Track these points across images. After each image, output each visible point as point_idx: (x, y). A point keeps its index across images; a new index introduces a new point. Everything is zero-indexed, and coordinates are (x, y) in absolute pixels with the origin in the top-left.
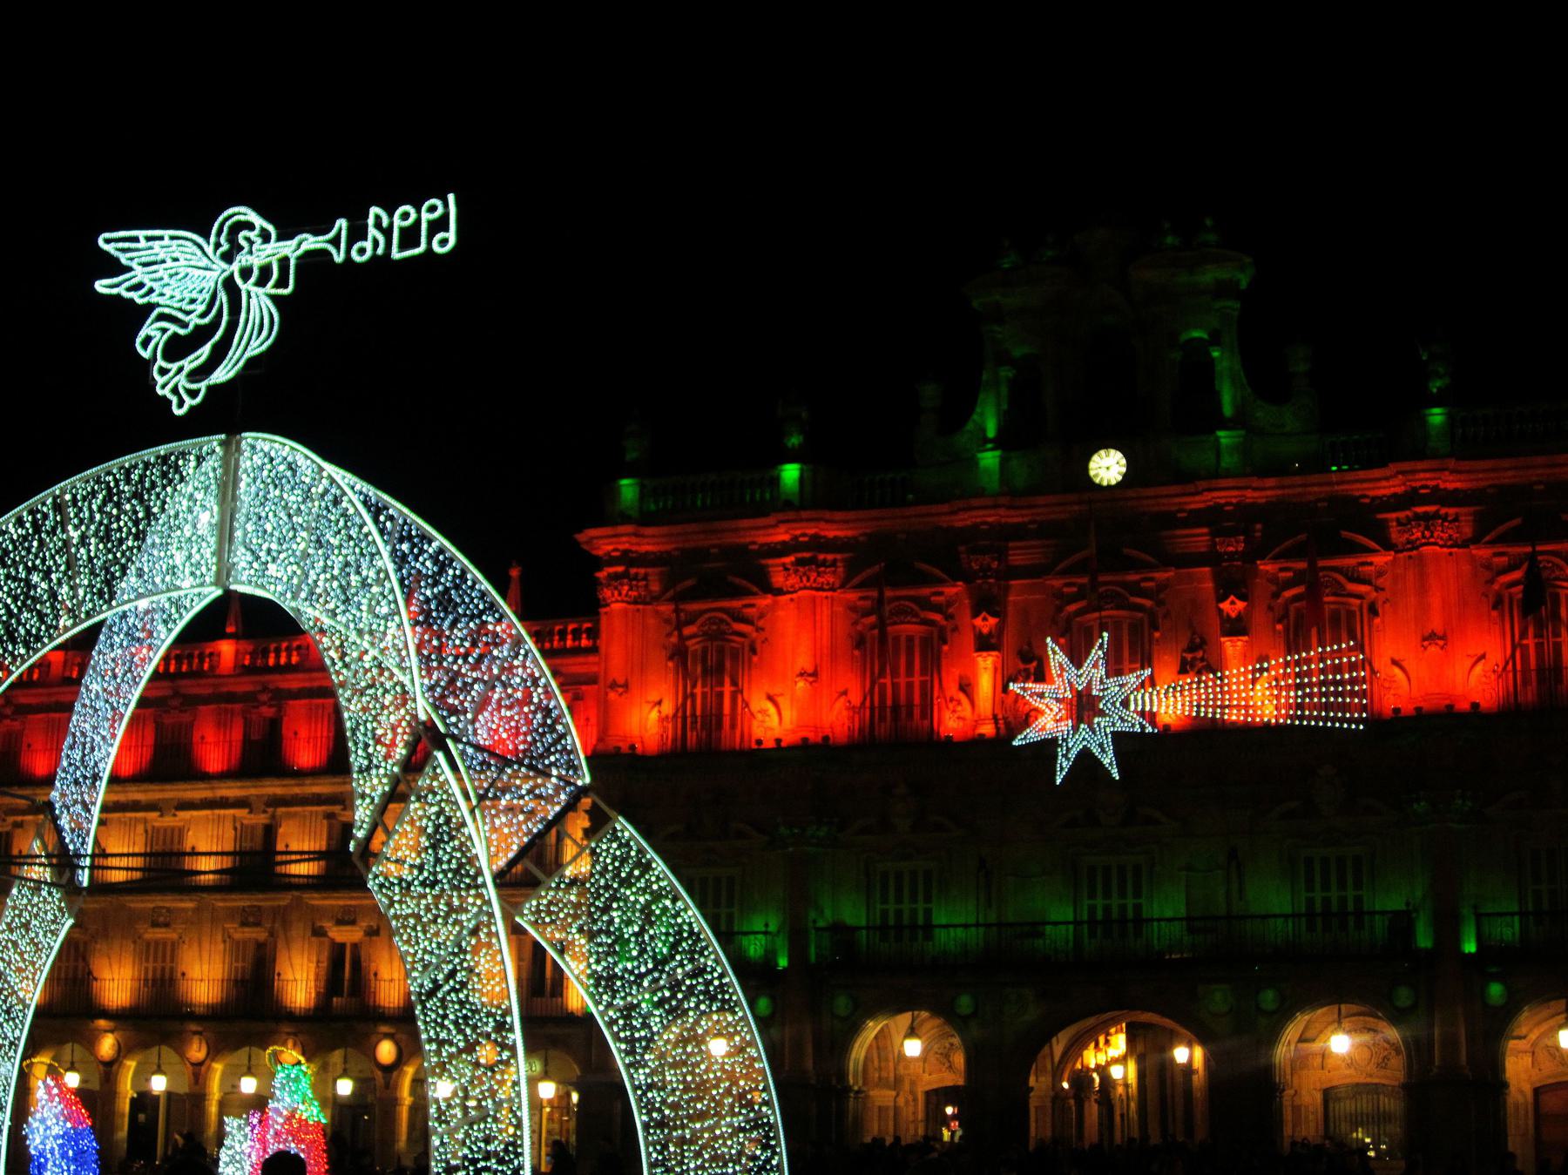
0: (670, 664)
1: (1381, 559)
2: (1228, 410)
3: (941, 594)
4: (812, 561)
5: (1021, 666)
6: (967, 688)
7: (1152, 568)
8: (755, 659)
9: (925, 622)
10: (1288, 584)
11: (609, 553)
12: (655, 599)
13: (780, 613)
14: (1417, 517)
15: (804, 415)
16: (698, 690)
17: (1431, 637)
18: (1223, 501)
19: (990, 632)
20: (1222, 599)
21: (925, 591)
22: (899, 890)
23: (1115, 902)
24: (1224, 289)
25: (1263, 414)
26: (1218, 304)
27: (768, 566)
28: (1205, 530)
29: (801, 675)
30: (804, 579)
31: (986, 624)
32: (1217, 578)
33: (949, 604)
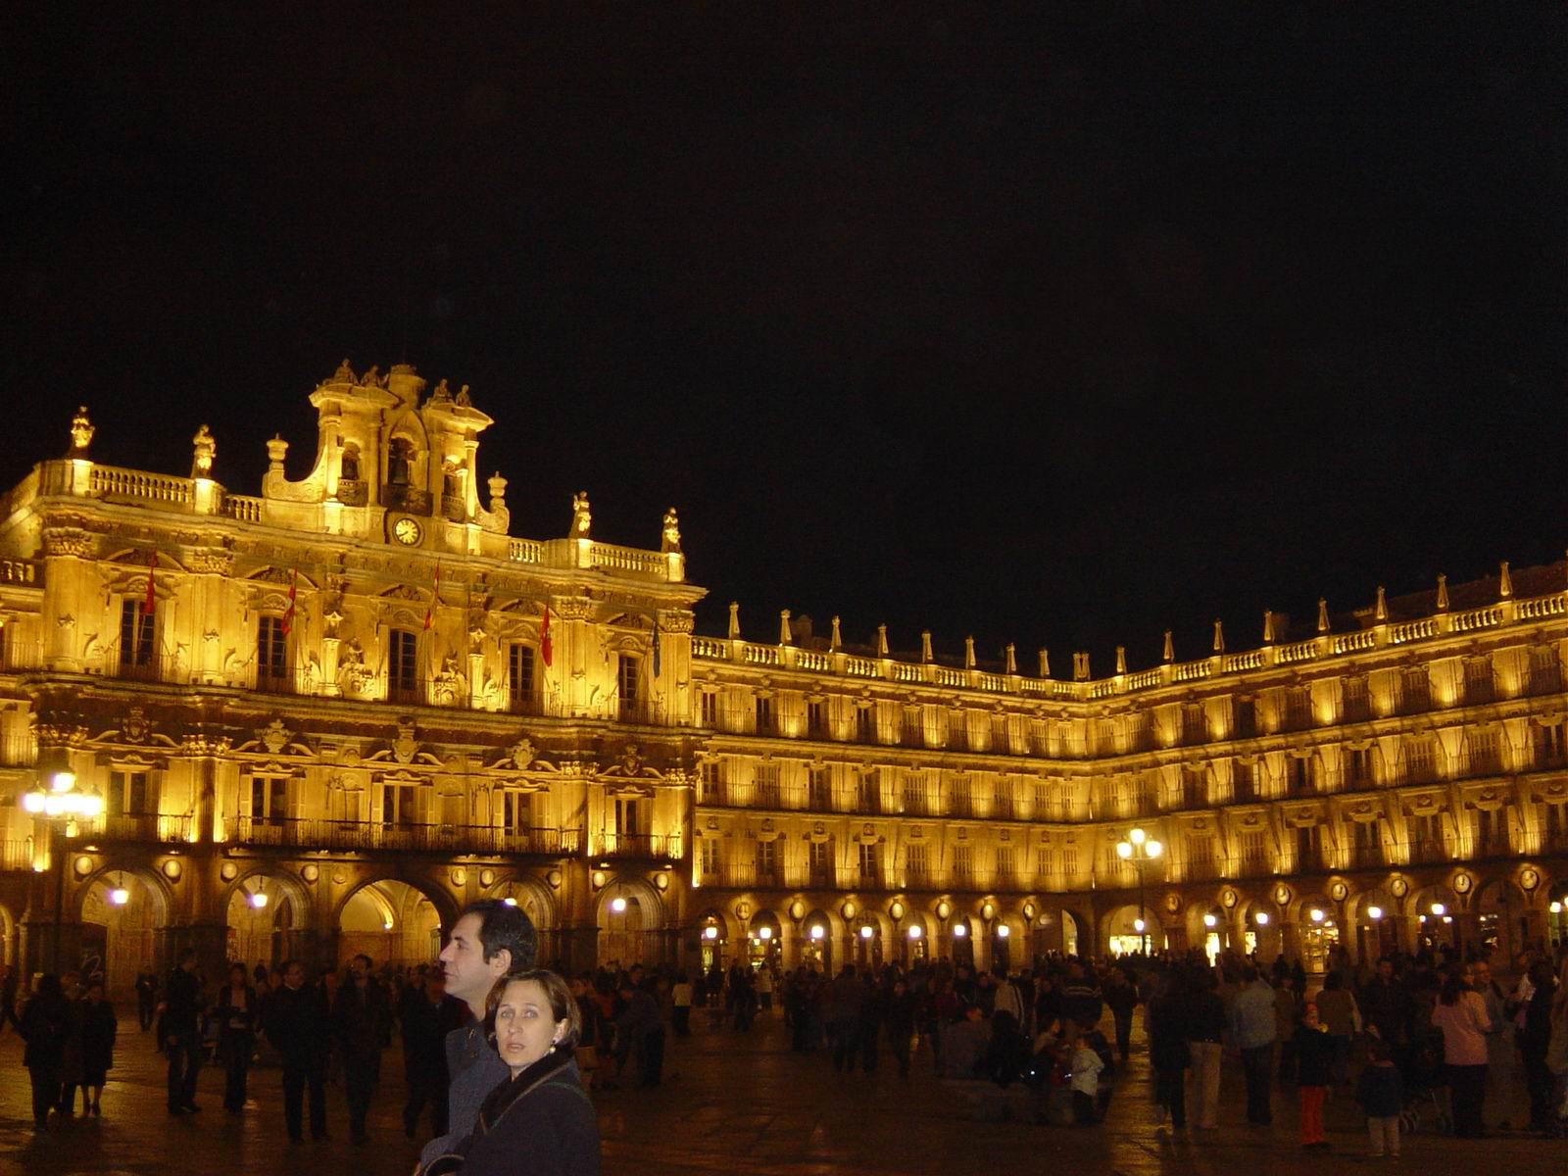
2: (471, 512)
5: (352, 650)
6: (314, 658)
10: (505, 627)
11: (68, 516)
14: (578, 602)
15: (213, 446)
17: (582, 673)
18: (476, 569)
20: (471, 630)
24: (470, 435)
26: (466, 443)
27: (183, 550)
28: (460, 584)
29: (214, 634)
30: (217, 566)
31: (335, 619)
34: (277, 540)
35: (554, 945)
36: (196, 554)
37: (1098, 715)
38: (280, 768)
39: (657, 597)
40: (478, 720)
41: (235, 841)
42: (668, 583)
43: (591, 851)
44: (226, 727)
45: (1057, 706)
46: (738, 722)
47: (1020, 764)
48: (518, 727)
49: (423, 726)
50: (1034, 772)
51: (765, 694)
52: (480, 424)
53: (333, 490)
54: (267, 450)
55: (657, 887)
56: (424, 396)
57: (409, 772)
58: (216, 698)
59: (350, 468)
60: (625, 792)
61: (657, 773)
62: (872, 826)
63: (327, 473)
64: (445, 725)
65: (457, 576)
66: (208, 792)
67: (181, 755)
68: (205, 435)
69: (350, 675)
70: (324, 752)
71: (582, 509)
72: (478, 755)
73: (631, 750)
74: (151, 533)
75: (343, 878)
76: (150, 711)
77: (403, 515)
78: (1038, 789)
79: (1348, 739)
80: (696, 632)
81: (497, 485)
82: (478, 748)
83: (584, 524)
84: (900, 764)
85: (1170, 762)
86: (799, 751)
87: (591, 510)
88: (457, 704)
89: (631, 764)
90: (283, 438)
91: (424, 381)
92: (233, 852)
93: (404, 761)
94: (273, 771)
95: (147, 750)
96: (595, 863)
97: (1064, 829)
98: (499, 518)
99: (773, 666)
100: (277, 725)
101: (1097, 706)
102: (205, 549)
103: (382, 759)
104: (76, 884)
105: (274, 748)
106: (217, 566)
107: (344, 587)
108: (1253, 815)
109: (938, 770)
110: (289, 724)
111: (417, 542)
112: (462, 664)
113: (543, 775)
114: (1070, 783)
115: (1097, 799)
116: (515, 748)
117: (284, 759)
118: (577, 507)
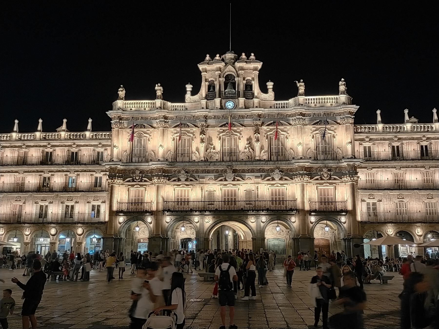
1: (288, 127)
2: (256, 94)
3: (192, 130)
7: (239, 126)
9: (188, 136)
10: (269, 131)
14: (297, 118)
19: (204, 139)
21: (189, 129)
24: (255, 69)
25: (263, 96)
30: (162, 125)
36: (157, 123)
39: (335, 112)
40: (256, 164)
44: (166, 174)
48: (274, 165)
49: (237, 168)
51: (396, 144)
53: (204, 95)
54: (186, 88)
55: (341, 222)
57: (232, 184)
60: (324, 186)
61: (338, 178)
63: (203, 91)
67: (153, 184)
70: (200, 180)
71: (300, 86)
72: (260, 177)
73: (325, 170)
75: (208, 221)
77: (228, 100)
81: (270, 85)
82: (259, 174)
93: (230, 181)
94: (183, 187)
95: (141, 183)
98: (271, 94)
100: (183, 172)
103: (221, 180)
105: (183, 179)
106: (162, 125)
113: (286, 182)
116: (273, 174)
117: (187, 183)
118: (298, 85)
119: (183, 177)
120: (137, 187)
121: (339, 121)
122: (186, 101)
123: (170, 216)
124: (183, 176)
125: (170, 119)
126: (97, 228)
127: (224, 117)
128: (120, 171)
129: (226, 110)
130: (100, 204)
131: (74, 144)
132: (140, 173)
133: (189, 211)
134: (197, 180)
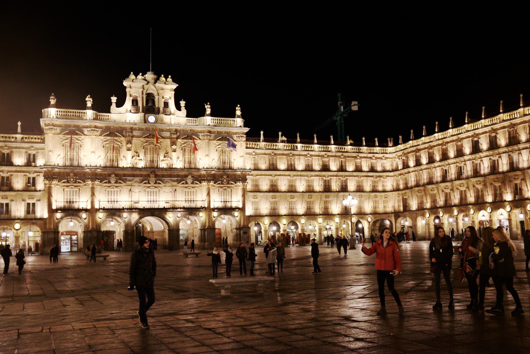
0: (63, 147)
2: (172, 112)
4: (94, 130)
5: (135, 154)
7: (160, 138)
8: (81, 148)
12: (60, 134)
13: (86, 140)
16: (69, 153)
17: (208, 155)
20: (173, 145)
22: (111, 194)
23: (152, 197)
29: (93, 152)
31: (129, 146)
32: (170, 141)
33: (121, 141)
34: (111, 124)
35: (201, 233)
37: (395, 158)
38: (115, 187)
41: (100, 209)
42: (236, 127)
43: (212, 207)
45: (381, 156)
46: (263, 166)
47: (366, 174)
49: (158, 173)
50: (372, 176)
52: (175, 86)
54: (111, 100)
55: (234, 216)
56: (156, 81)
58: (93, 170)
59: (135, 102)
61: (233, 183)
62: (311, 195)
63: (128, 104)
64: (165, 173)
65: (167, 130)
66: (93, 194)
67: (86, 185)
68: (89, 98)
69: (135, 160)
70: (128, 182)
73: (225, 177)
74: (75, 126)
75: (135, 217)
76: (75, 175)
78: (374, 182)
79: (458, 163)
80: (247, 140)
81: (183, 103)
82: (175, 179)
83: (208, 111)
84: (321, 176)
85: (412, 172)
86: (285, 174)
87: (211, 108)
88: (169, 167)
89: (225, 181)
90: (115, 96)
91: (156, 76)
92: (101, 211)
93: (152, 184)
95: (75, 184)
96: (213, 210)
97: (384, 194)
98: (184, 112)
99: (276, 149)
100: (113, 176)
101: (394, 155)
102: (90, 129)
103: (145, 183)
104: (57, 221)
105: (113, 181)
107: (133, 136)
108: (433, 188)
109: (335, 178)
110: (116, 175)
111: (156, 121)
112: (170, 155)
113: (197, 185)
114: (386, 180)
115: (395, 184)
118: (206, 107)
119: (113, 181)
120: (72, 188)
121: (235, 139)
122: (111, 111)
123: (103, 213)
124: (113, 179)
125: (99, 128)
126: (33, 224)
127: (147, 130)
128: (54, 174)
129: (149, 124)
130: (34, 202)
131: (6, 146)
132: (74, 176)
133: (121, 209)
134: (125, 182)
